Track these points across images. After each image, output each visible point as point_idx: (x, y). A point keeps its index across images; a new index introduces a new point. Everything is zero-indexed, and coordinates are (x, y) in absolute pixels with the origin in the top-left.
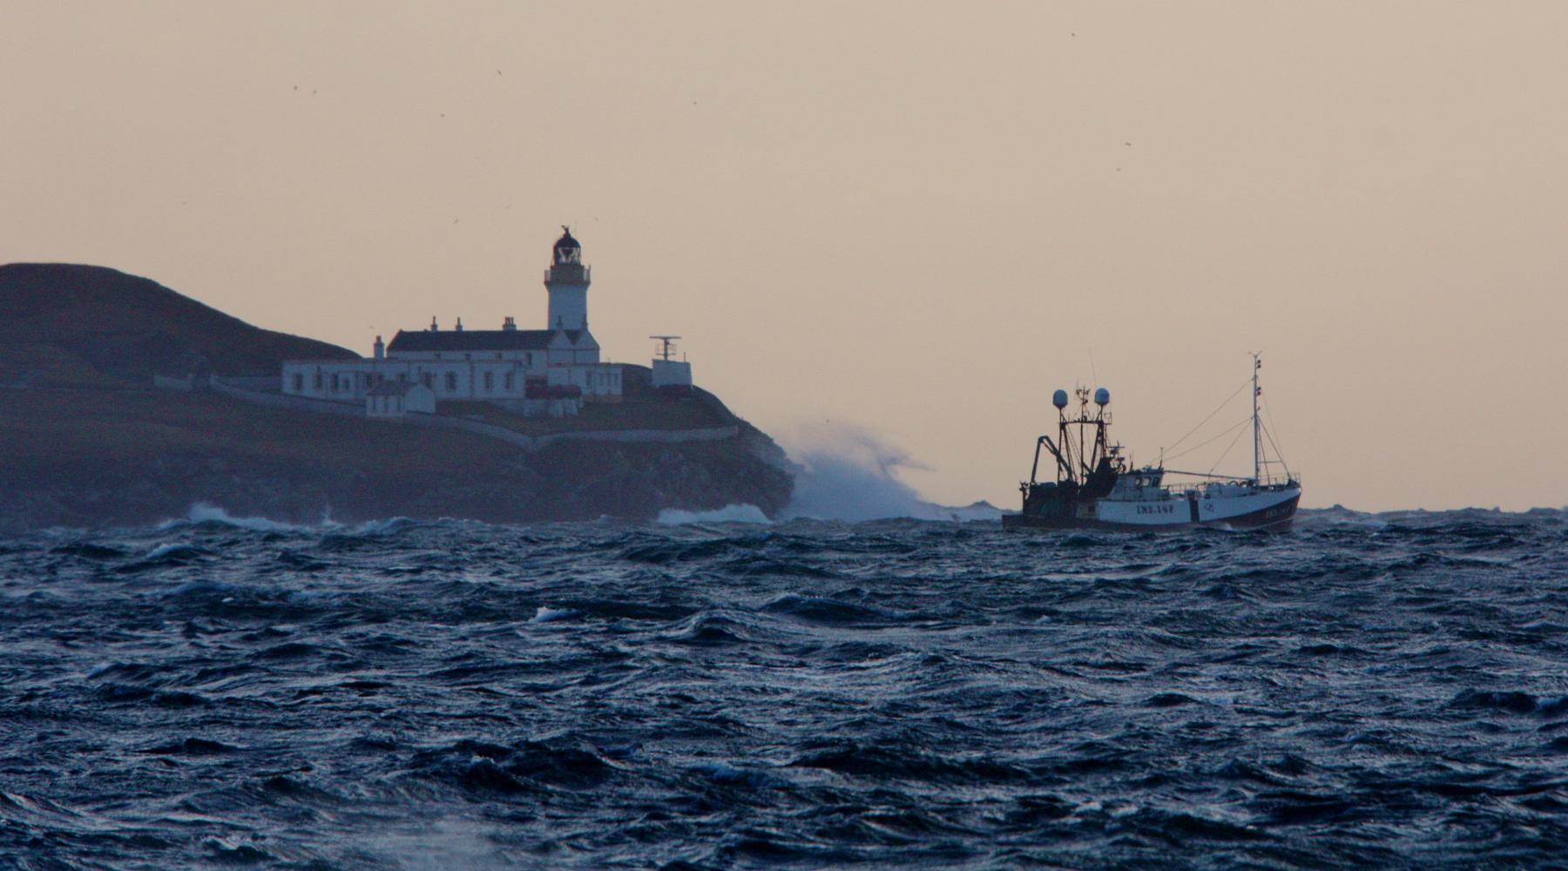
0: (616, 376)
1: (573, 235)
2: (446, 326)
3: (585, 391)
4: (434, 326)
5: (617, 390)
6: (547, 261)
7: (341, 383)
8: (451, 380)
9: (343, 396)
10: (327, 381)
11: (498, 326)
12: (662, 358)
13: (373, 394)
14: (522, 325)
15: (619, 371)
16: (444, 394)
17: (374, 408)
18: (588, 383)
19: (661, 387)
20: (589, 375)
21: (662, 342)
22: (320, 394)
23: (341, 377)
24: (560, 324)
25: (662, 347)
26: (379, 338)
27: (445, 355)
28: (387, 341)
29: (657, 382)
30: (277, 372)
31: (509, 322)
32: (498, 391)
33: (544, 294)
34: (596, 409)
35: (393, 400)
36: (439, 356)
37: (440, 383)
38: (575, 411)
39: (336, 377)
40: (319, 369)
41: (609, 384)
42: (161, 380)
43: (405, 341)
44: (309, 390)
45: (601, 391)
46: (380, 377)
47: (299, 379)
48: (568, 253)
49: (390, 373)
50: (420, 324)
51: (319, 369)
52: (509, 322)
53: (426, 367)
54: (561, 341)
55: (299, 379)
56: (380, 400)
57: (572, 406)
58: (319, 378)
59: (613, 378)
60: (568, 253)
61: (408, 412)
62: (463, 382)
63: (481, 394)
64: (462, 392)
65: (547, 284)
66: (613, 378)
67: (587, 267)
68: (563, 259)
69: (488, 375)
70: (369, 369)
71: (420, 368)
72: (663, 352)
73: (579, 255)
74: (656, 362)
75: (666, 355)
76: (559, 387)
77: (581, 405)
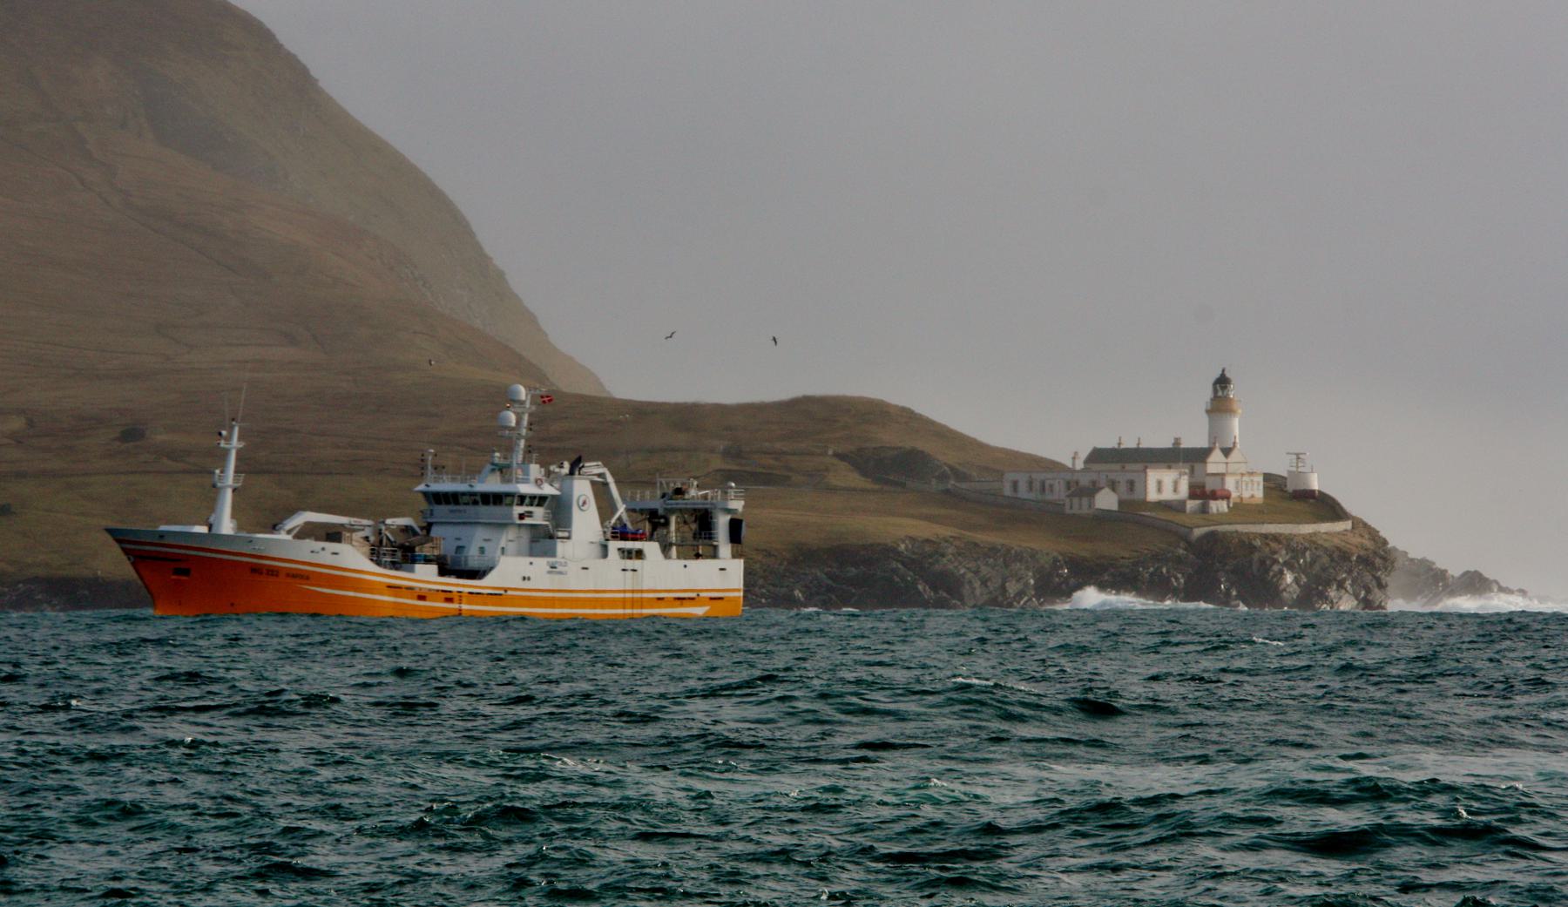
0: (1258, 484)
1: (1228, 375)
2: (1129, 443)
3: (1234, 495)
4: (1119, 444)
6: (1208, 393)
8: (1131, 484)
9: (1048, 497)
10: (1037, 485)
11: (1167, 443)
12: (1294, 469)
13: (1068, 496)
14: (1185, 445)
15: (1261, 479)
16: (1126, 497)
17: (1071, 508)
18: (1237, 488)
19: (1295, 491)
20: (1237, 482)
21: (1295, 457)
22: (1032, 496)
23: (1047, 483)
25: (1295, 461)
26: (1076, 453)
27: (1129, 467)
28: (1084, 455)
29: (1290, 488)
31: (1177, 441)
32: (1168, 495)
33: (1205, 419)
34: (1242, 510)
35: (1085, 501)
36: (1124, 467)
37: (1123, 488)
38: (1226, 510)
39: (1043, 484)
41: (1252, 490)
43: (1097, 456)
44: (1023, 493)
45: (1246, 495)
46: (1077, 483)
47: (1015, 485)
49: (1085, 481)
50: (1109, 443)
52: (1177, 441)
53: (1112, 476)
54: (1217, 455)
55: (1015, 485)
56: (1076, 500)
58: (1030, 483)
59: (1256, 485)
62: (1138, 486)
64: (1137, 496)
65: (1208, 412)
66: (1256, 485)
68: (1220, 394)
69: (1159, 483)
70: (1068, 477)
74: (1289, 472)
75: (1297, 467)
77: (1231, 505)
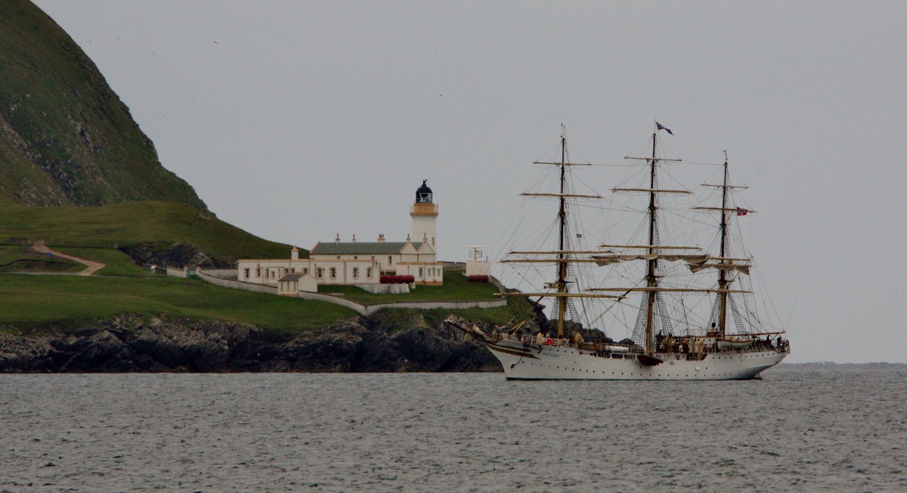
3: (418, 279)
4: (338, 240)
5: (440, 279)
7: (270, 273)
10: (263, 272)
17: (282, 289)
18: (421, 274)
20: (421, 270)
22: (259, 281)
23: (270, 270)
24: (408, 239)
30: (235, 267)
32: (362, 280)
34: (423, 290)
35: (292, 283)
38: (408, 291)
40: (258, 266)
42: (171, 272)
44: (253, 278)
45: (429, 279)
46: (293, 270)
47: (247, 270)
48: (424, 196)
51: (258, 266)
53: (319, 265)
56: (285, 284)
57: (405, 288)
59: (436, 272)
60: (424, 196)
61: (300, 291)
63: (350, 280)
64: (339, 280)
66: (436, 272)
67: (436, 205)
69: (355, 270)
71: (315, 265)
72: (473, 256)
73: (431, 198)
76: (400, 277)
77: (414, 287)
